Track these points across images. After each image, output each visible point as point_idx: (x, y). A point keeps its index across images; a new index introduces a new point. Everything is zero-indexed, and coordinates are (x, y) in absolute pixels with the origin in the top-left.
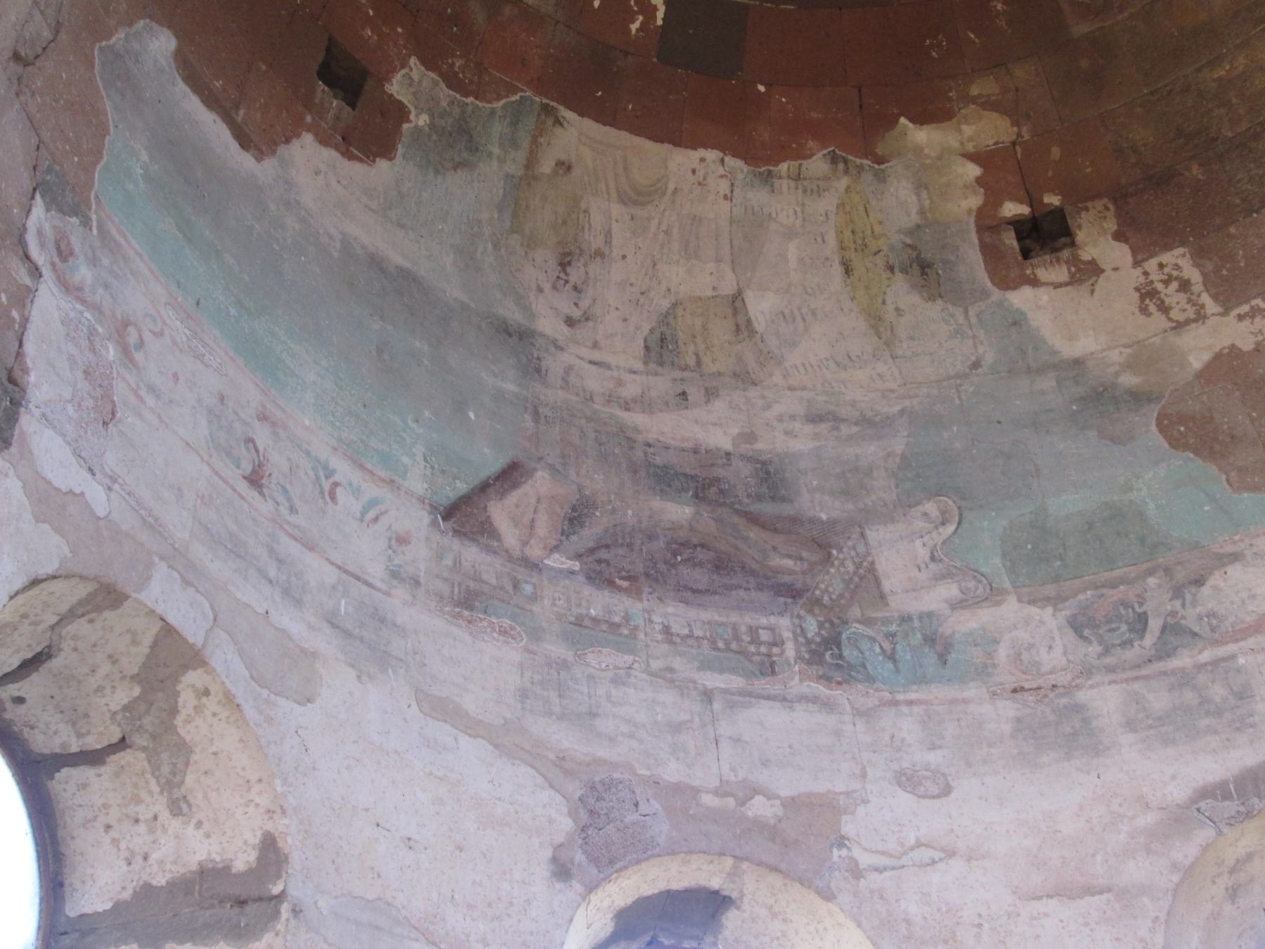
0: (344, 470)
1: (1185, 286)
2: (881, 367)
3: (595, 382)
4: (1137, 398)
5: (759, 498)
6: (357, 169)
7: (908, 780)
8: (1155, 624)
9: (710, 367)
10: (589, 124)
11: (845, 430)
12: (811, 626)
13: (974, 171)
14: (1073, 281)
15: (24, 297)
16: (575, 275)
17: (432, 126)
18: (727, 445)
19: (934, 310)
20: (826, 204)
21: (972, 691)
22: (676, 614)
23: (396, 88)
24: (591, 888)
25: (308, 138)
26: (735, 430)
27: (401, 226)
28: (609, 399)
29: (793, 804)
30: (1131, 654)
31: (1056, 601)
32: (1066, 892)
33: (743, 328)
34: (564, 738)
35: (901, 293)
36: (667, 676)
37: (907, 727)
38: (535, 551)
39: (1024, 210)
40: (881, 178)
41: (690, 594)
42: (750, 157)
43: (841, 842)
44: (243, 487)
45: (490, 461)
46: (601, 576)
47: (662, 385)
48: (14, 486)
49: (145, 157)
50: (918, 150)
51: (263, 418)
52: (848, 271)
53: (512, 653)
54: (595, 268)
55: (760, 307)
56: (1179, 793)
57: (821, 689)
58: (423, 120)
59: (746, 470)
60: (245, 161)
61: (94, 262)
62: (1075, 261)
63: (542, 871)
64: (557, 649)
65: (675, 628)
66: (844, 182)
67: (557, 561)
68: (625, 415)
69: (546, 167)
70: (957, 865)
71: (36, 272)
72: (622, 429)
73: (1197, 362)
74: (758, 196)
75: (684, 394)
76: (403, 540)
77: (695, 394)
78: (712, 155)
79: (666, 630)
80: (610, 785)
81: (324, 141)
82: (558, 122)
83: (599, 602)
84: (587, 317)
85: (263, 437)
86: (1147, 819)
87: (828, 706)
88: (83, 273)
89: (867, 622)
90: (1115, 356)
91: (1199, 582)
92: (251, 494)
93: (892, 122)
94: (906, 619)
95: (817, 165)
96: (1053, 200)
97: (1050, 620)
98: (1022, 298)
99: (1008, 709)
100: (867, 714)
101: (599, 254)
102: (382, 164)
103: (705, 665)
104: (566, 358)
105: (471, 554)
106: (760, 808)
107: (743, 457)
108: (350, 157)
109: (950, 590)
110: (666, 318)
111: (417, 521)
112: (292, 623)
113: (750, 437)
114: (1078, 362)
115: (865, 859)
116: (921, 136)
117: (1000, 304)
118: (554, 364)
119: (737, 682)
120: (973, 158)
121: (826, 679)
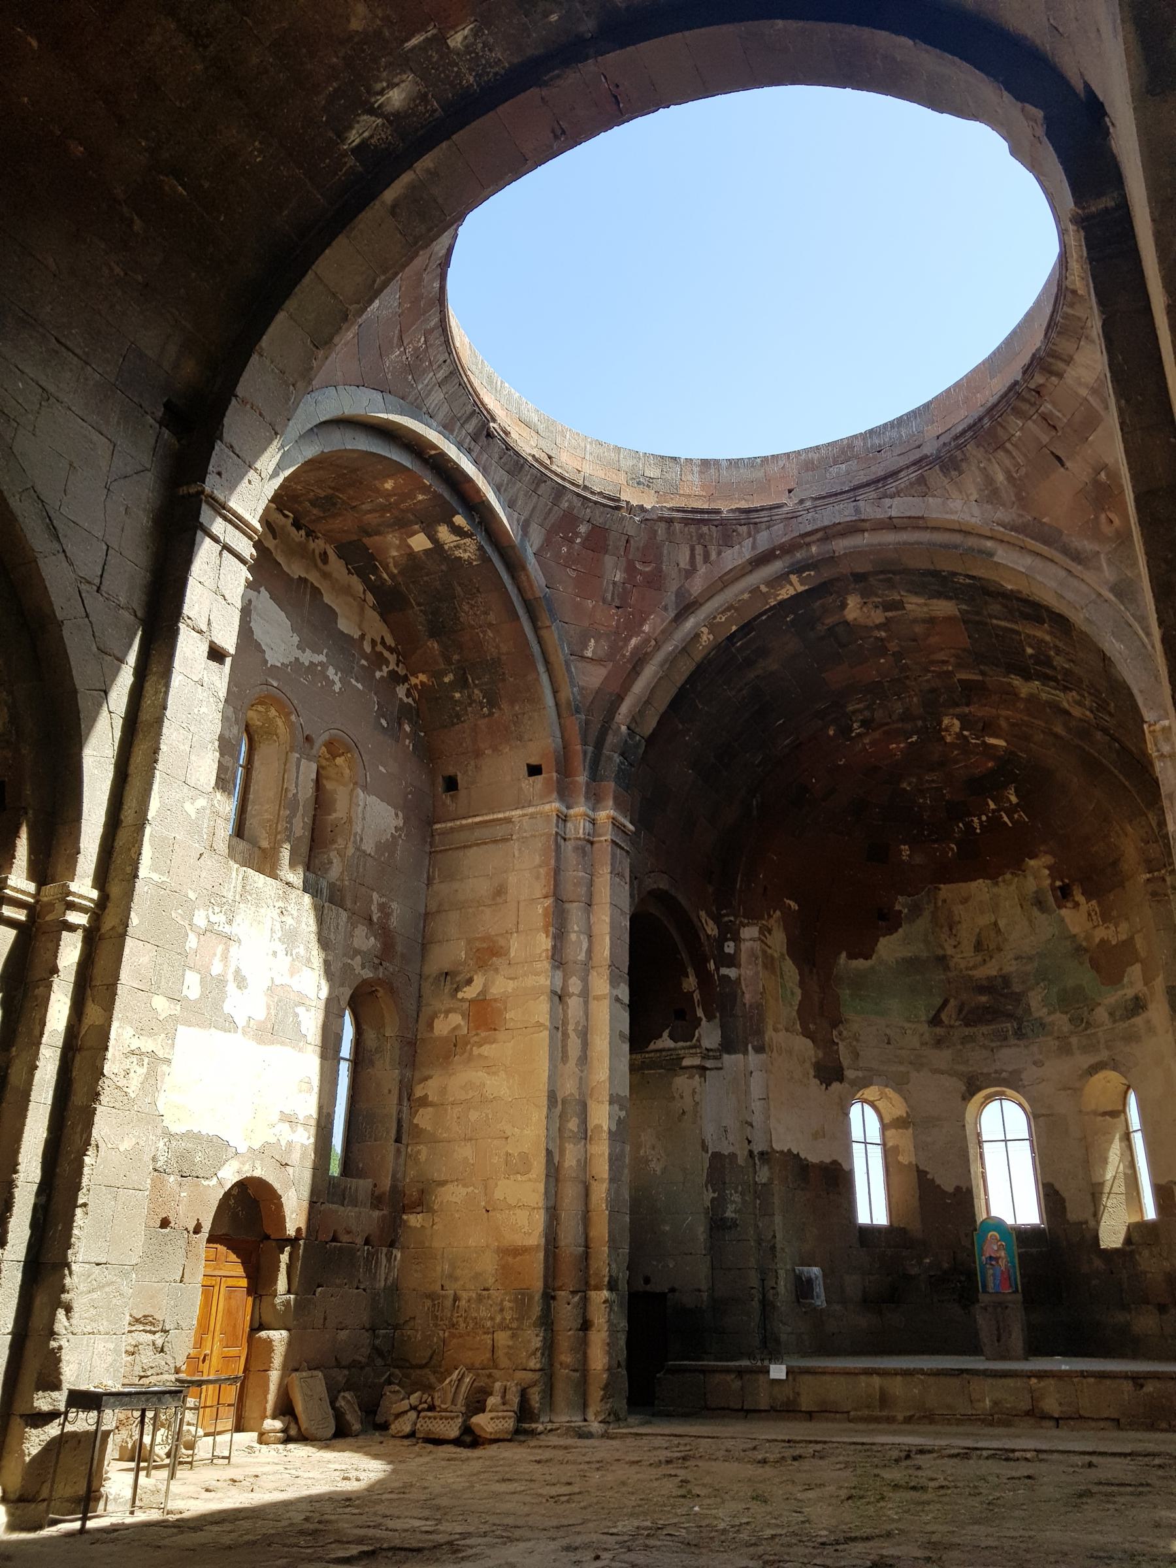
0: (907, 1025)
1: (1096, 914)
2: (1032, 938)
3: (963, 965)
4: (1086, 950)
5: (1003, 988)
6: (895, 935)
7: (1035, 1063)
8: (1085, 1021)
9: (991, 948)
10: (949, 886)
11: (1024, 961)
12: (1015, 1025)
13: (1047, 872)
14: (1074, 908)
15: (837, 1051)
16: (954, 932)
17: (909, 910)
18: (995, 973)
19: (1045, 916)
20: (1013, 887)
21: (1049, 1038)
22: (984, 1029)
23: (897, 907)
24: (969, 1100)
25: (881, 939)
26: (997, 968)
27: (909, 944)
28: (967, 969)
29: (1011, 1073)
30: (1080, 1028)
31: (1066, 1013)
32: (1065, 1089)
33: (999, 931)
34: (962, 1068)
35: (1036, 912)
36: (984, 1047)
37: (1035, 1048)
38: (952, 1022)
39: (1060, 884)
40: (1025, 877)
41: (989, 1022)
42: (990, 879)
43: (1021, 1080)
44: (886, 1046)
45: (938, 1001)
46: (967, 1025)
47: (979, 958)
48: (847, 1085)
49: (848, 991)
50: (1032, 867)
51: (887, 1026)
52: (1022, 907)
53: (950, 1051)
54: (959, 926)
55: (1002, 923)
56: (1085, 1066)
57: (1016, 1042)
58: (906, 911)
59: (1000, 980)
60: (869, 963)
61: (846, 1029)
62: (1073, 900)
63: (960, 1099)
64: (960, 1047)
65: (986, 1033)
66: (1016, 879)
67: (957, 1023)
68: (970, 972)
69: (940, 903)
70: (1044, 1083)
71: (837, 1044)
72: (969, 975)
73: (1097, 940)
74: (995, 890)
75: (985, 960)
76: (922, 1035)
77: (987, 959)
78: (981, 881)
79: (983, 1034)
80: (973, 1076)
81: (884, 936)
82: (939, 889)
83: (967, 1031)
84: (959, 943)
85: (888, 1031)
86: (1080, 1072)
87: (1018, 1046)
88: (845, 1033)
89: (1028, 1021)
90: (1082, 935)
91: (1093, 1010)
92: (890, 1046)
93: (1024, 860)
94: (1036, 1019)
95: (1008, 876)
96: (1067, 881)
97: (1065, 1018)
98: (1064, 912)
99: (1057, 1043)
100: (1026, 1047)
101: (959, 922)
102: (900, 930)
103: (992, 1041)
104: (955, 960)
105: (939, 1030)
106: (1004, 1075)
107: (1000, 976)
108: (891, 934)
109: (1045, 1010)
110: (979, 934)
111: (924, 1028)
112: (902, 1068)
113: (1001, 969)
114: (1075, 936)
115: (1026, 1083)
116: (1032, 863)
117: (1059, 914)
118: (952, 964)
119: (999, 1043)
120: (1045, 867)
121: (1018, 1039)
